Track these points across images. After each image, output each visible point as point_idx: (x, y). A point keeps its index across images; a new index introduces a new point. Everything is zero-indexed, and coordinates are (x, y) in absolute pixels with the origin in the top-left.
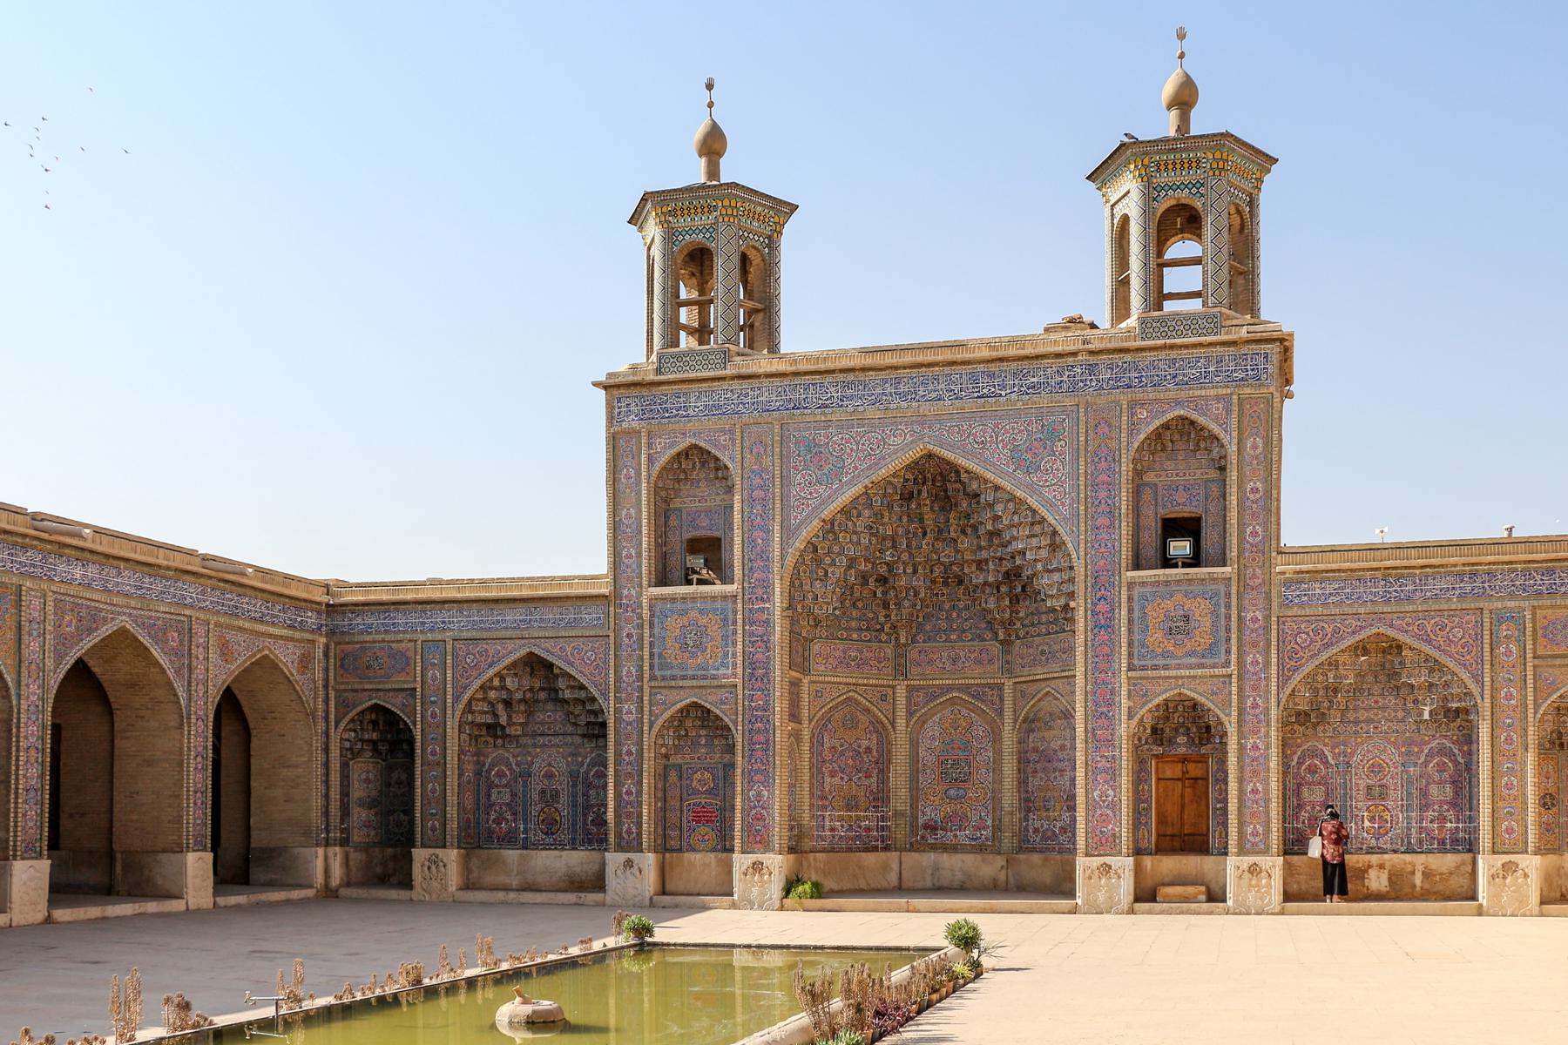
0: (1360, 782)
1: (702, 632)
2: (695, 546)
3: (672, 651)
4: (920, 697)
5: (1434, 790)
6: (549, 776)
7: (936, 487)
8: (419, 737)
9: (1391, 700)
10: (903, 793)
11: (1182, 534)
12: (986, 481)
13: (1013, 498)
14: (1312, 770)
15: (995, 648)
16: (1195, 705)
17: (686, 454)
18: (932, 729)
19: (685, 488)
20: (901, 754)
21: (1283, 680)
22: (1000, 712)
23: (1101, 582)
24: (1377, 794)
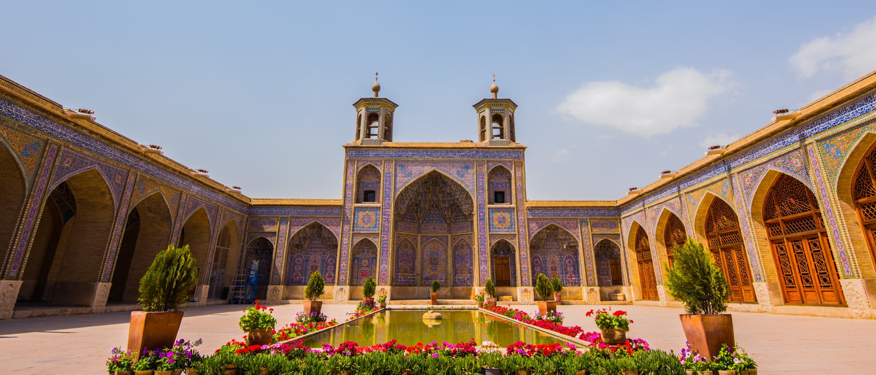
0: (549, 266)
1: (369, 217)
3: (360, 222)
4: (424, 239)
5: (568, 268)
6: (315, 261)
7: (435, 180)
8: (275, 247)
9: (555, 243)
10: (419, 268)
11: (499, 197)
13: (456, 183)
14: (537, 262)
15: (446, 226)
16: (506, 243)
17: (367, 167)
18: (427, 249)
19: (365, 176)
20: (419, 256)
21: (530, 236)
22: (447, 244)
23: (481, 207)
24: (554, 269)
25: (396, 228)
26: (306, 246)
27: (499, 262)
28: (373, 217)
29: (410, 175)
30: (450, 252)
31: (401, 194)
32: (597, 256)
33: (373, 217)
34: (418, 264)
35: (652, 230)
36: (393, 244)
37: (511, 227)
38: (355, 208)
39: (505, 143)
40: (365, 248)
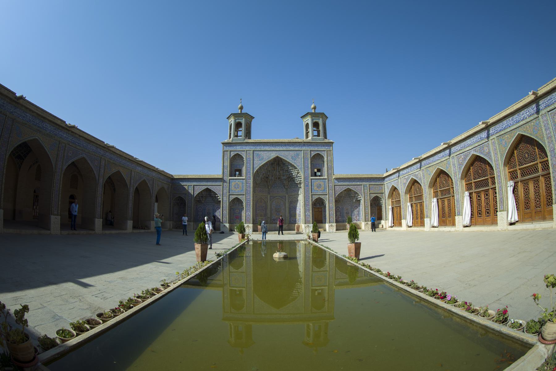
1: (238, 185)
2: (236, 170)
3: (232, 188)
7: (278, 162)
10: (269, 214)
12: (286, 161)
15: (285, 190)
25: (254, 191)
26: (203, 202)
27: (317, 210)
28: (241, 185)
29: (262, 159)
30: (287, 205)
31: (257, 171)
32: (371, 205)
33: (241, 185)
34: (268, 212)
35: (402, 189)
36: (253, 200)
37: (324, 190)
38: (230, 180)
39: (321, 139)
40: (236, 204)
